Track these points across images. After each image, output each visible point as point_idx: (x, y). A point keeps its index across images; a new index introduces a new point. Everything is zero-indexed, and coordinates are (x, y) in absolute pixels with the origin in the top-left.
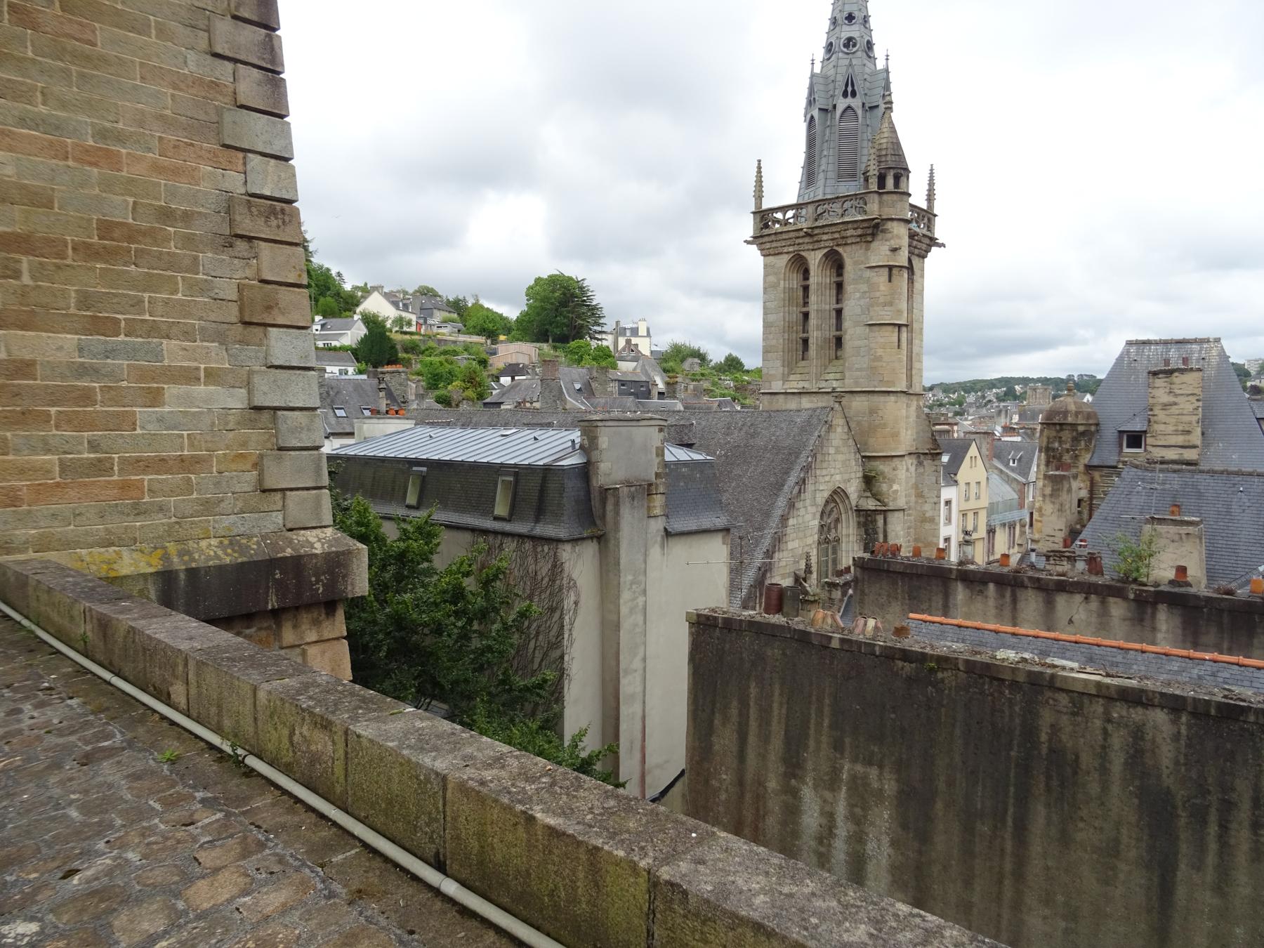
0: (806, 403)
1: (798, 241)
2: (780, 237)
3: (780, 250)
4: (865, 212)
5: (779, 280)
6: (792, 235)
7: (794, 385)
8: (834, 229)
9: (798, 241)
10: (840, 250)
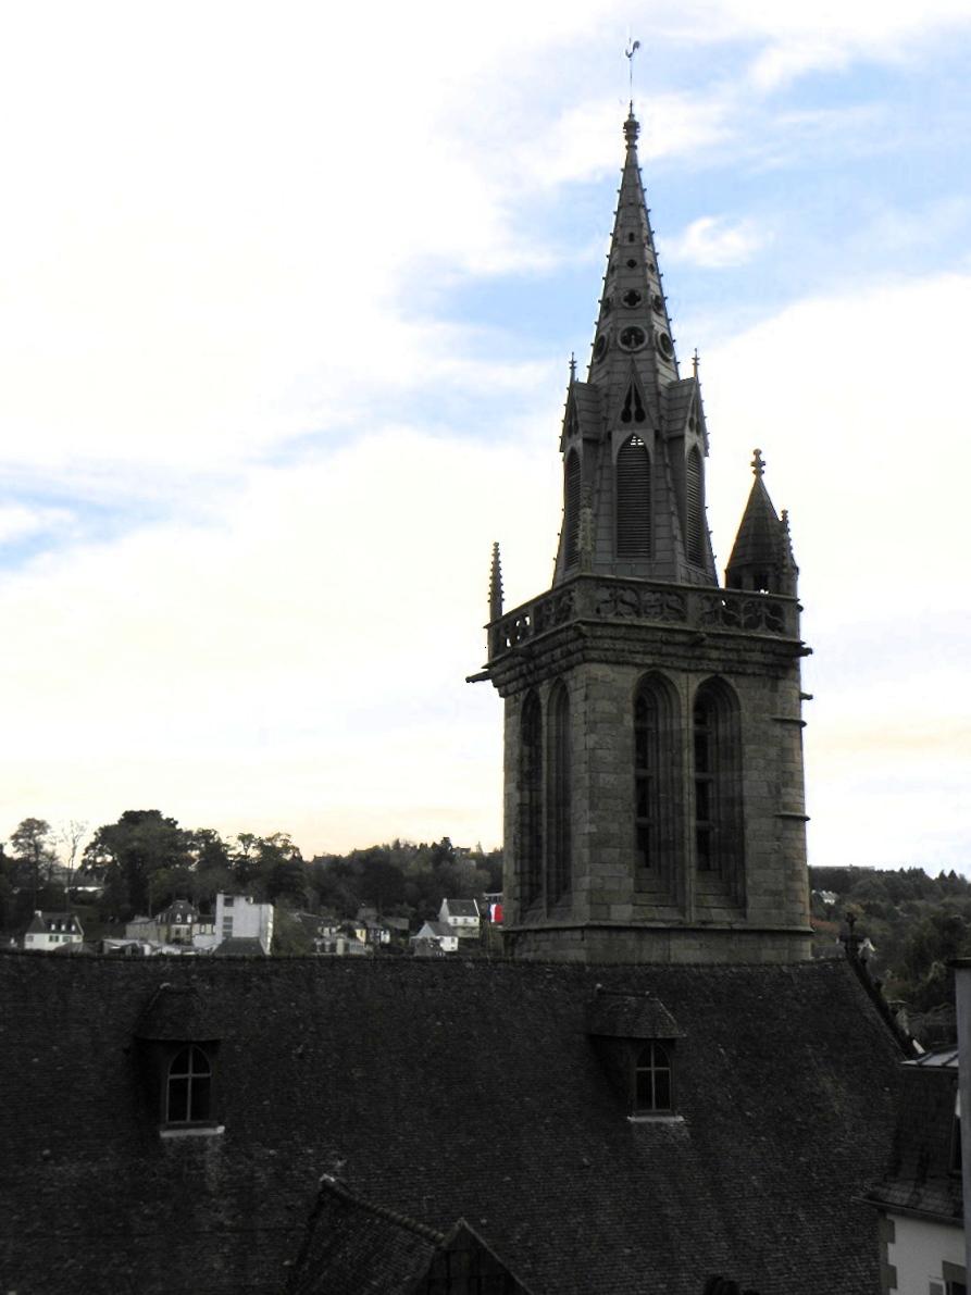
1: (665, 649)
3: (629, 658)
4: (781, 630)
5: (622, 711)
8: (730, 644)
9: (665, 649)
10: (732, 681)
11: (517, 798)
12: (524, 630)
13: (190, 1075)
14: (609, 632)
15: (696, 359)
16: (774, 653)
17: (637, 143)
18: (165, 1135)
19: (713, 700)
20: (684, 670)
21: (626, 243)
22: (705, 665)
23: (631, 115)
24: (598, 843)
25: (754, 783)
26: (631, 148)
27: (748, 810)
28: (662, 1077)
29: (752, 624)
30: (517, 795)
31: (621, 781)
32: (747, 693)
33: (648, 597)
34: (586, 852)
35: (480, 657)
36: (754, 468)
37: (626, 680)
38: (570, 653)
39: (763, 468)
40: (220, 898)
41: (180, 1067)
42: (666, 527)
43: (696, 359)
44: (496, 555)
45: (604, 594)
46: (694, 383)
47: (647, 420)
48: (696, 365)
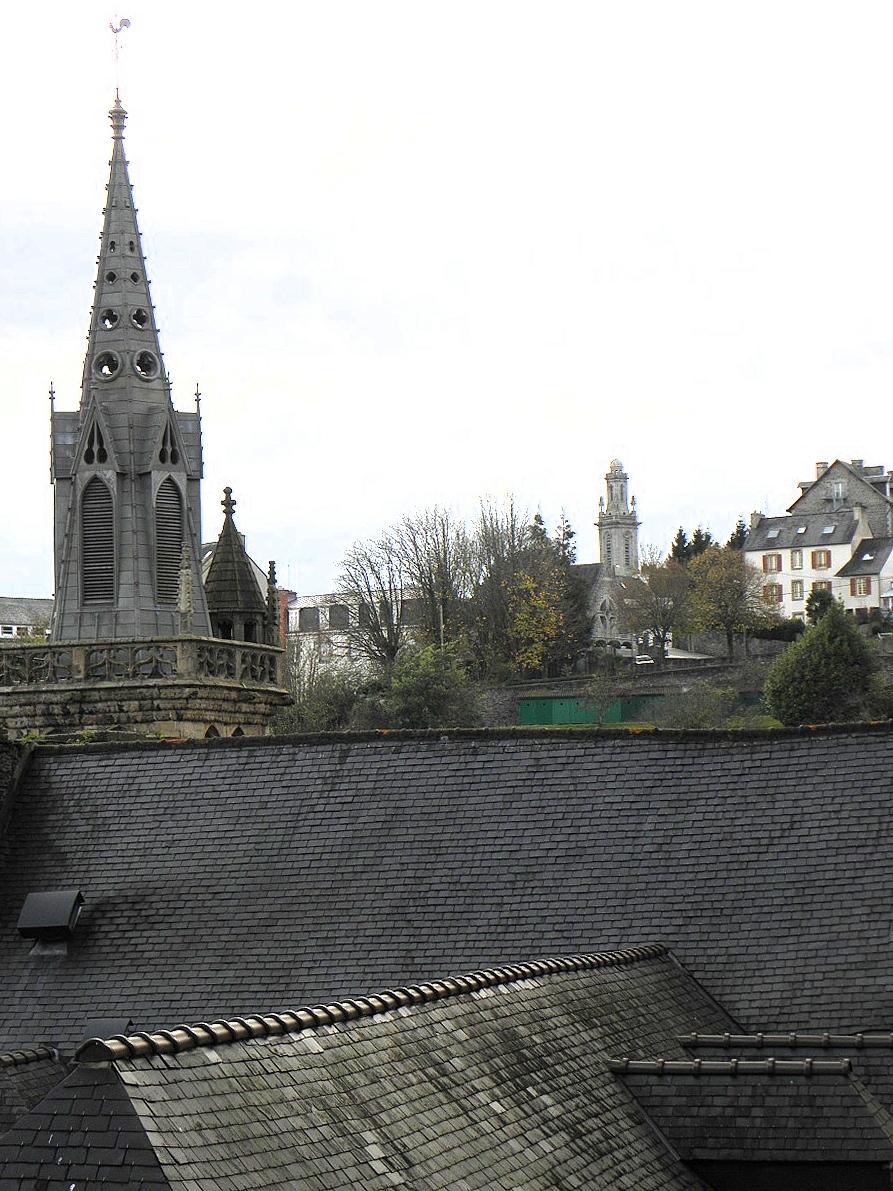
15: (198, 395)
16: (271, 704)
17: (124, 133)
20: (226, 724)
21: (129, 253)
23: (118, 101)
26: (118, 139)
36: (224, 508)
38: (159, 709)
39: (234, 507)
43: (198, 395)
46: (196, 418)
47: (180, 461)
48: (198, 400)
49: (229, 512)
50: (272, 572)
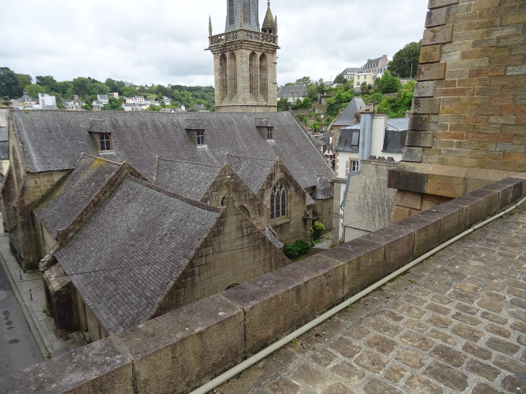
0: (258, 110)
1: (256, 47)
2: (251, 43)
3: (249, 48)
6: (255, 43)
7: (255, 103)
8: (267, 46)
10: (266, 54)
11: (219, 77)
12: (222, 40)
13: (200, 136)
14: (246, 42)
18: (198, 147)
19: (263, 57)
22: (262, 50)
24: (244, 88)
25: (269, 76)
27: (268, 82)
28: (271, 133)
29: (270, 41)
30: (219, 77)
31: (247, 75)
32: (268, 55)
33: (253, 34)
34: (242, 90)
35: (207, 44)
37: (249, 53)
40: (40, 95)
41: (198, 134)
42: (253, 18)
44: (210, 20)
45: (245, 33)
49: (269, 6)
50: (276, 18)
